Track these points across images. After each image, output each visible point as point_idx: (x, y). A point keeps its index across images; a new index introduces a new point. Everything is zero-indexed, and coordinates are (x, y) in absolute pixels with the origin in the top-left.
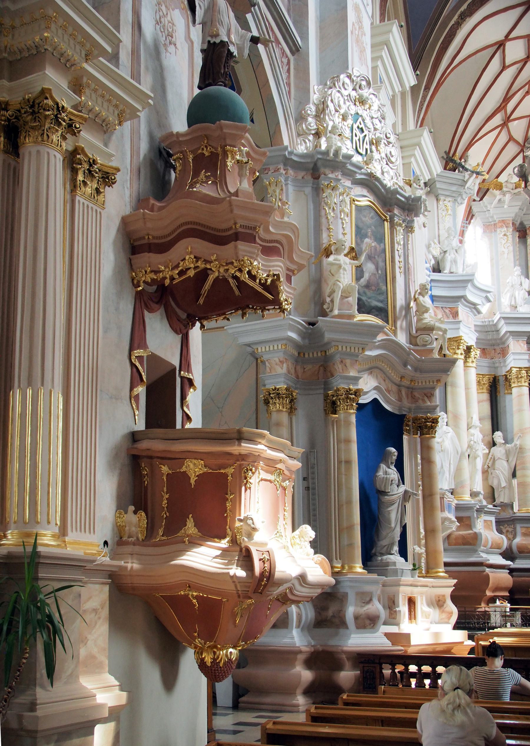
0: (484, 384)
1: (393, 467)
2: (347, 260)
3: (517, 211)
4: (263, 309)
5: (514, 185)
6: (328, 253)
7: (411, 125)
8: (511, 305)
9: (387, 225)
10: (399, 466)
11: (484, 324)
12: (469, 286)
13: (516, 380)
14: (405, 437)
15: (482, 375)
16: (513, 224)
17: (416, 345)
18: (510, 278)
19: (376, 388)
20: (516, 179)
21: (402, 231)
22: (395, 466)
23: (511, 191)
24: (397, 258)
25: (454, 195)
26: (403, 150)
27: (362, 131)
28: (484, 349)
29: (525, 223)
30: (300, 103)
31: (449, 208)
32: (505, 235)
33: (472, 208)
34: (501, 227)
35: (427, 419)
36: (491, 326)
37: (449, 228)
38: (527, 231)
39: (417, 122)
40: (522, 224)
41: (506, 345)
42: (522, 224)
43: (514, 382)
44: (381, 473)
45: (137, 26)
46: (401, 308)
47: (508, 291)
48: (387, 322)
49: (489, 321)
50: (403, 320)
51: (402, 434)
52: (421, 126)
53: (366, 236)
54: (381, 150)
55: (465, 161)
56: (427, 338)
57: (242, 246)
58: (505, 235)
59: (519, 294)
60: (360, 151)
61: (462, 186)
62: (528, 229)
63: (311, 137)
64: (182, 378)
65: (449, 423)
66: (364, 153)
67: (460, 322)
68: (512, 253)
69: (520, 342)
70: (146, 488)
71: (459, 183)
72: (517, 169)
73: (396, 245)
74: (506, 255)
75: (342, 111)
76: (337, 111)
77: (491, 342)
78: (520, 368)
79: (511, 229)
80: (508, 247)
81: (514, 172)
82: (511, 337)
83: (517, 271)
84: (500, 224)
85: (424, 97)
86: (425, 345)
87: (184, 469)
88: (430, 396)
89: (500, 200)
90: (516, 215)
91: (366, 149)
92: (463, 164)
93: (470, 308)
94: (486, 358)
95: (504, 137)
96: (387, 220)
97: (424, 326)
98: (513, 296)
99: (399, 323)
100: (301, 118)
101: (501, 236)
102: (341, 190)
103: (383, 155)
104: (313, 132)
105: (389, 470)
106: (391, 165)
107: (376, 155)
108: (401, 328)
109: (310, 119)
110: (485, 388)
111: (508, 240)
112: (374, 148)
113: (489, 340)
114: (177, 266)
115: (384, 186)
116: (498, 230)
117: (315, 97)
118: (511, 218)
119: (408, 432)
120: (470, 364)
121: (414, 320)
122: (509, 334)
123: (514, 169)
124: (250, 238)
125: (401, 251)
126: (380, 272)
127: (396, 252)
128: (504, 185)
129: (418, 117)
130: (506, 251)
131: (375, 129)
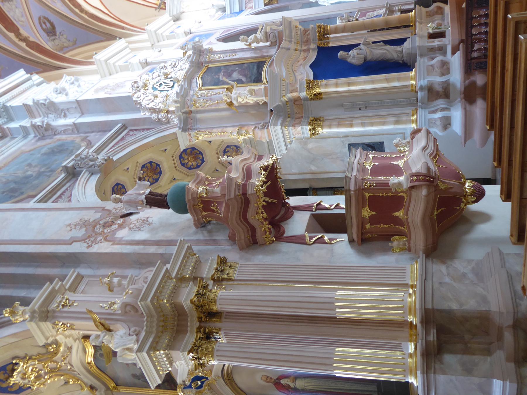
2: (234, 92)
4: (277, 169)
6: (231, 104)
7: (144, 36)
10: (348, 48)
14: (331, 45)
21: (212, 56)
24: (228, 58)
26: (159, 40)
27: (161, 84)
30: (152, 122)
45: (144, 243)
46: (255, 53)
48: (265, 62)
53: (218, 79)
54: (169, 72)
56: (272, 36)
57: (249, 192)
63: (169, 115)
64: (316, 209)
66: (172, 82)
70: (378, 235)
73: (221, 59)
75: (153, 98)
76: (153, 101)
85: (128, 29)
87: (367, 218)
91: (171, 81)
99: (265, 54)
100: (159, 121)
102: (195, 97)
104: (166, 114)
106: (177, 65)
107: (173, 75)
108: (267, 52)
109: (160, 117)
112: (169, 76)
114: (262, 223)
115: (189, 69)
117: (147, 114)
119: (328, 43)
121: (262, 44)
124: (244, 187)
126: (237, 68)
127: (225, 58)
131: (159, 76)
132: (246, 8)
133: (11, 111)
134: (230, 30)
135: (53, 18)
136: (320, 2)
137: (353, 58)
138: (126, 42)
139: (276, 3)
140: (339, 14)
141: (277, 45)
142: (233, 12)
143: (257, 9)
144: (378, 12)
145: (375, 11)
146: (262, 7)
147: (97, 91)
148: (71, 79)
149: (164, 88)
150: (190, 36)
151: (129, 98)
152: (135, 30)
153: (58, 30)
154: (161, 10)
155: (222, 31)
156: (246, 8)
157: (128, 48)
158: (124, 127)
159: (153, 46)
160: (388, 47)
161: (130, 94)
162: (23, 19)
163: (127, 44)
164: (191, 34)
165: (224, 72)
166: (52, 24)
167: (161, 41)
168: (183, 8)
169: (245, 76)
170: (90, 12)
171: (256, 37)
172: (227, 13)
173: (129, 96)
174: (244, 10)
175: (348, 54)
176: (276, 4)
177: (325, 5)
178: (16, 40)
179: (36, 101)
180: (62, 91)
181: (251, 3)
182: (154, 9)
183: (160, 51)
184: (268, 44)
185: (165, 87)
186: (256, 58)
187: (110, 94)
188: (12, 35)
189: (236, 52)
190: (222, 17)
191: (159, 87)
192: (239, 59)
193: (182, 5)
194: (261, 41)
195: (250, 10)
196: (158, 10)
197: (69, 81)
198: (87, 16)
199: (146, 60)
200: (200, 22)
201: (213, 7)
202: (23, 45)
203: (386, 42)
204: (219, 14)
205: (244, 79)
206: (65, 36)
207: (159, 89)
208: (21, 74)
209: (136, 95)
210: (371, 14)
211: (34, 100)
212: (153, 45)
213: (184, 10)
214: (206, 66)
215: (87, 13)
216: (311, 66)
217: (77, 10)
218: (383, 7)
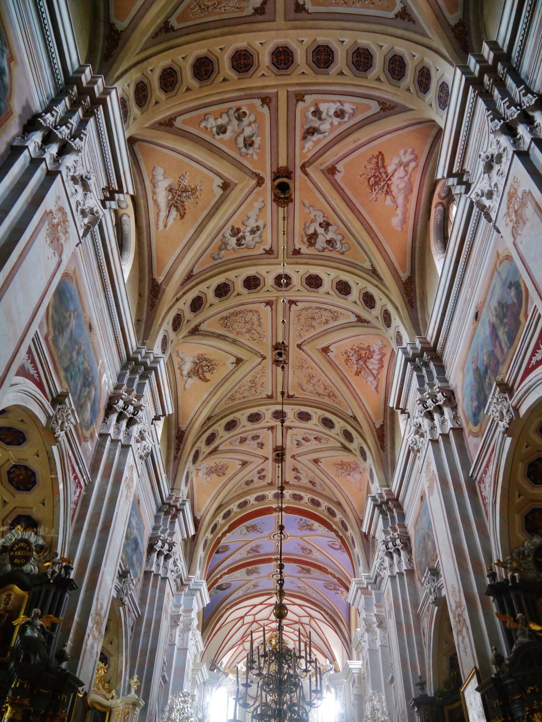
95: (241, 648)
100: (163, 711)
117: (169, 701)
133: (190, 598)
135: (228, 591)
147: (189, 660)
151: (181, 688)
153: (220, 592)
158: (165, 681)
162: (233, 576)
166: (225, 589)
178: (222, 573)
188: (226, 571)
202: (218, 576)
206: (214, 594)
208: (207, 601)
209: (181, 695)
215: (225, 612)
217: (229, 606)
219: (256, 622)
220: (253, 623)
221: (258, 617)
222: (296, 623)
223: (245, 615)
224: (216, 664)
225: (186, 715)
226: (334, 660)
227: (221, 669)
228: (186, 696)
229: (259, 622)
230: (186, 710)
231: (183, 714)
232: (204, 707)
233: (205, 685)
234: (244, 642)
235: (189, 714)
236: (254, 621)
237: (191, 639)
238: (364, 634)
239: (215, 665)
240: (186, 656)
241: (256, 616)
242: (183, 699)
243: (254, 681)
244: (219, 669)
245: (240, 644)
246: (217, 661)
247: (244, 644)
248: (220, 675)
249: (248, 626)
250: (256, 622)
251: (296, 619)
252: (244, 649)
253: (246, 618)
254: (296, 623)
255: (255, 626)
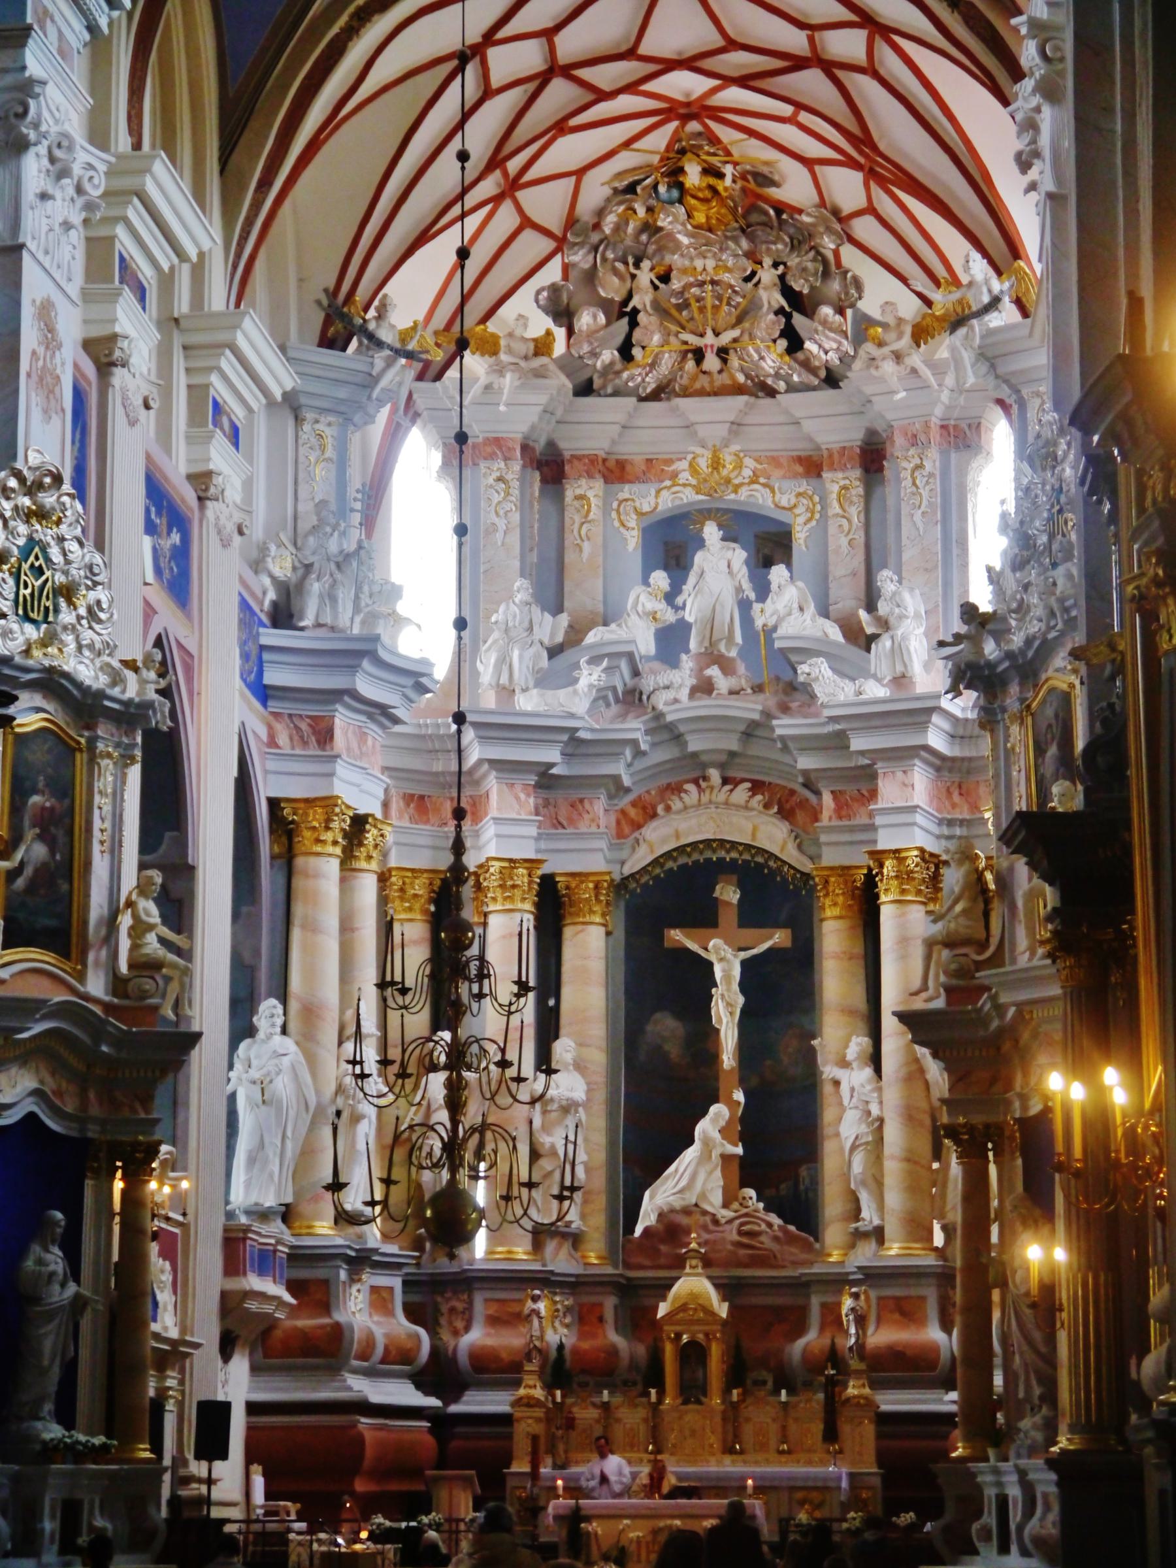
0: (416, 896)
1: (56, 1250)
3: (535, 419)
5: (532, 346)
8: (498, 685)
9: (80, 759)
11: (423, 732)
12: (366, 664)
13: (499, 891)
15: (412, 870)
16: (525, 448)
17: (126, 996)
18: (502, 608)
19: (37, 1093)
20: (540, 323)
22: (61, 1248)
23: (523, 364)
24: (97, 824)
25: (342, 409)
28: (422, 797)
29: (562, 445)
31: (329, 442)
32: (500, 479)
33: (415, 396)
34: (491, 457)
35: (136, 1145)
36: (443, 736)
37: (323, 504)
38: (567, 468)
39: (235, 267)
40: (551, 445)
41: (483, 791)
42: (551, 445)
43: (494, 899)
44: (29, 1263)
47: (495, 642)
49: (438, 726)
50: (100, 948)
51: (84, 1177)
52: (238, 305)
53: (35, 791)
54: (78, 603)
55: (380, 317)
56: (148, 985)
58: (500, 479)
59: (521, 657)
60: (34, 616)
61: (364, 386)
62: (570, 461)
65: (292, 1027)
66: (40, 618)
67: (338, 756)
68: (518, 531)
69: (518, 788)
71: (359, 379)
72: (545, 294)
73: (97, 799)
74: (499, 536)
77: (442, 779)
78: (511, 860)
79: (517, 466)
80: (506, 513)
81: (537, 301)
82: (494, 773)
83: (521, 590)
84: (489, 449)
85: (256, 206)
86: (143, 998)
88: (146, 1100)
89: (488, 387)
90: (533, 428)
92: (372, 326)
93: (370, 716)
94: (427, 822)
95: (506, 218)
96: (81, 750)
97: (143, 959)
98: (504, 660)
99: (91, 957)
101: (491, 480)
103: (82, 611)
105: (49, 1257)
106: (97, 627)
108: (97, 963)
110: (417, 906)
111: (508, 494)
113: (437, 774)
115: (78, 685)
116: (483, 465)
118: (520, 436)
120: (363, 864)
121: (124, 944)
122: (486, 766)
123: (538, 293)
125: (107, 809)
126: (58, 857)
127: (96, 812)
128: (503, 342)
129: (238, 255)
130: (501, 524)
132: (276, 715)
134: (189, 680)
136: (249, 1048)
137: (40, 1262)
138: (201, 255)
139: (276, 849)
140: (186, 1160)
141: (116, 1000)
142: (266, 656)
143: (263, 765)
144: (171, 1308)
145: (175, 1292)
146: (265, 789)
147: (45, 310)
148: (97, 187)
149: (26, 587)
150: (188, 495)
152: (248, 233)
154: (322, 315)
155: (192, 647)
156: (276, 715)
157: (176, 260)
159: (173, 323)
160: (55, 1373)
161: (19, 465)
163: (194, 259)
164: (200, 499)
165: (52, 809)
167: (186, 357)
168: (317, 422)
169: (31, 887)
170: (350, 44)
171: (151, 927)
172: (268, 635)
173: (14, 457)
174: (265, 705)
175: (53, 1242)
176: (271, 849)
177: (231, 1067)
179: (37, 90)
180: (58, 166)
181: (291, 739)
182: (331, 283)
183: (147, 407)
184: (124, 968)
185: (29, 591)
186: (85, 923)
187: (29, 375)
189: (112, 852)
190: (253, 613)
191: (32, 565)
192: (88, 864)
193: (331, 419)
194: (135, 947)
195: (263, 733)
196: (325, 302)
197: (91, 178)
198: (337, 35)
199: (123, 366)
200: (245, 530)
201: (297, 564)
203: (70, 1368)
204: (264, 593)
205: (20, 883)
207: (25, 567)
209: (13, 483)
210: (167, 1277)
211: (44, 83)
212: (176, 321)
213: (306, 427)
214: (79, 743)
216: (31, 1116)
218: (183, 1330)
219: (566, 71)
220: (543, 79)
221: (570, 44)
222: (797, 63)
223: (489, 38)
224: (354, 310)
225: (60, 578)
226: (1015, 250)
227: (385, 335)
228: (39, 486)
229: (584, 73)
230: (55, 553)
231: (39, 572)
232: (304, 526)
233: (298, 420)
234: (513, 186)
235: (77, 573)
236: (553, 70)
237: (44, 196)
238: (1038, 110)
239: (346, 319)
240: (17, 285)
241: (559, 39)
242: (26, 501)
243: (597, 383)
244: (371, 337)
245: (497, 200)
246: (361, 295)
247: (521, 195)
248: (379, 363)
249: (514, 97)
250: (566, 71)
251: (795, 41)
252: (526, 223)
253: (493, 53)
254: (797, 63)
255: (559, 93)
